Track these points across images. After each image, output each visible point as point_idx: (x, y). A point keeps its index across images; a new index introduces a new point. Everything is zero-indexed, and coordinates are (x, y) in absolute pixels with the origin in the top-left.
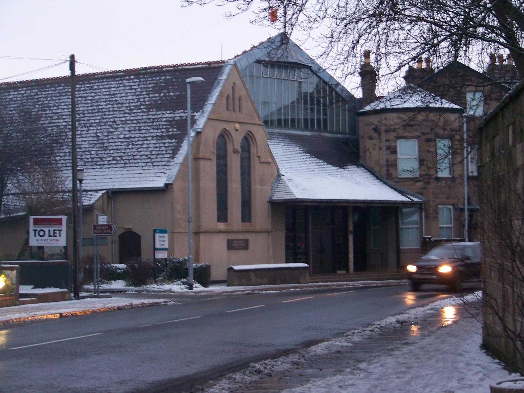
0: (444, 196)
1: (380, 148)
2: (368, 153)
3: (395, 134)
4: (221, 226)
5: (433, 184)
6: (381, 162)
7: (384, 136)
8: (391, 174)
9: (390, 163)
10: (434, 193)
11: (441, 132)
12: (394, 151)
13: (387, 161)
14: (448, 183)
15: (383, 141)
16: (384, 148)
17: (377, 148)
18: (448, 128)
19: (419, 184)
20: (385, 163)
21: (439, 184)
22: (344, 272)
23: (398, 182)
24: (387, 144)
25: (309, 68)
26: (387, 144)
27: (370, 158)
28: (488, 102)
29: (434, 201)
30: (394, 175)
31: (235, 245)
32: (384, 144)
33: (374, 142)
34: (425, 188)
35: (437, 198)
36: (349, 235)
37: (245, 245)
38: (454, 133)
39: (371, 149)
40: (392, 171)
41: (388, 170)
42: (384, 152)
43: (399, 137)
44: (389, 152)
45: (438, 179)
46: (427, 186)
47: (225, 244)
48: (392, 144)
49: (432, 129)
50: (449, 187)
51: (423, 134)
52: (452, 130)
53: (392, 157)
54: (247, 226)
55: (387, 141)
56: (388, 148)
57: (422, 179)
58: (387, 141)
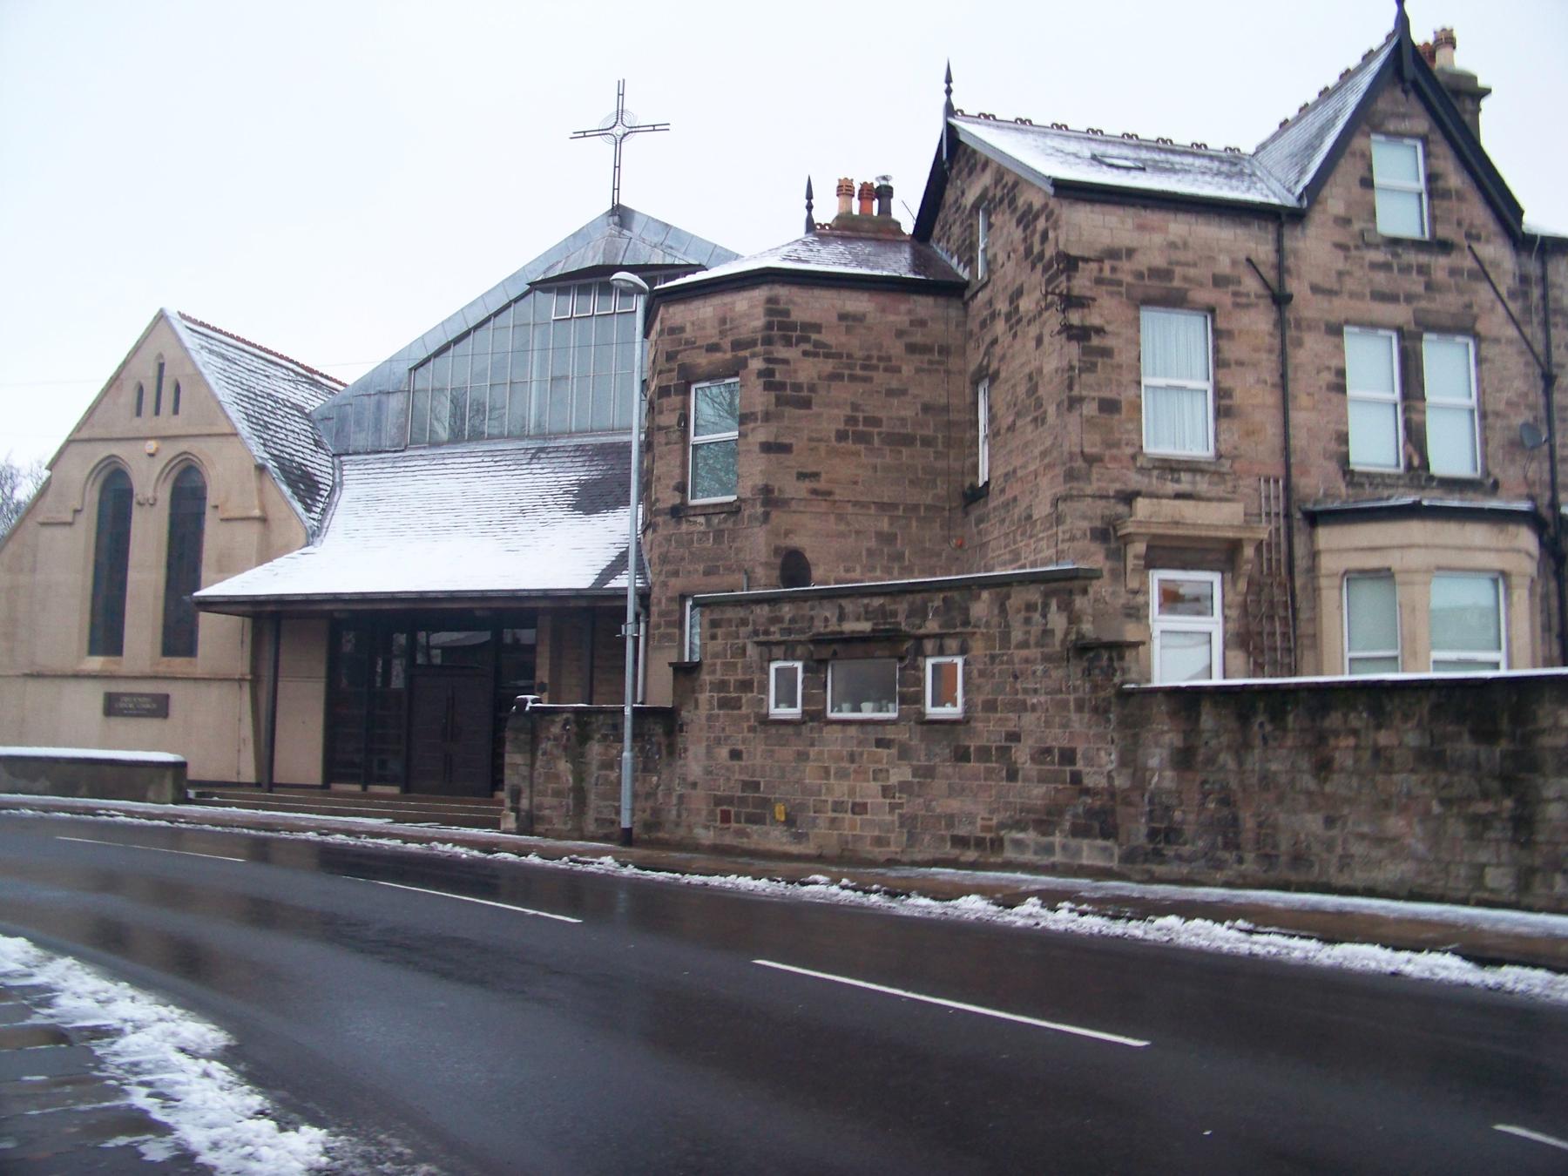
0: (701, 568)
4: (96, 663)
11: (702, 360)
14: (715, 520)
21: (684, 527)
29: (665, 584)
31: (122, 705)
35: (676, 574)
37: (160, 707)
38: (747, 353)
47: (98, 703)
50: (719, 535)
52: (737, 345)
54: (178, 664)
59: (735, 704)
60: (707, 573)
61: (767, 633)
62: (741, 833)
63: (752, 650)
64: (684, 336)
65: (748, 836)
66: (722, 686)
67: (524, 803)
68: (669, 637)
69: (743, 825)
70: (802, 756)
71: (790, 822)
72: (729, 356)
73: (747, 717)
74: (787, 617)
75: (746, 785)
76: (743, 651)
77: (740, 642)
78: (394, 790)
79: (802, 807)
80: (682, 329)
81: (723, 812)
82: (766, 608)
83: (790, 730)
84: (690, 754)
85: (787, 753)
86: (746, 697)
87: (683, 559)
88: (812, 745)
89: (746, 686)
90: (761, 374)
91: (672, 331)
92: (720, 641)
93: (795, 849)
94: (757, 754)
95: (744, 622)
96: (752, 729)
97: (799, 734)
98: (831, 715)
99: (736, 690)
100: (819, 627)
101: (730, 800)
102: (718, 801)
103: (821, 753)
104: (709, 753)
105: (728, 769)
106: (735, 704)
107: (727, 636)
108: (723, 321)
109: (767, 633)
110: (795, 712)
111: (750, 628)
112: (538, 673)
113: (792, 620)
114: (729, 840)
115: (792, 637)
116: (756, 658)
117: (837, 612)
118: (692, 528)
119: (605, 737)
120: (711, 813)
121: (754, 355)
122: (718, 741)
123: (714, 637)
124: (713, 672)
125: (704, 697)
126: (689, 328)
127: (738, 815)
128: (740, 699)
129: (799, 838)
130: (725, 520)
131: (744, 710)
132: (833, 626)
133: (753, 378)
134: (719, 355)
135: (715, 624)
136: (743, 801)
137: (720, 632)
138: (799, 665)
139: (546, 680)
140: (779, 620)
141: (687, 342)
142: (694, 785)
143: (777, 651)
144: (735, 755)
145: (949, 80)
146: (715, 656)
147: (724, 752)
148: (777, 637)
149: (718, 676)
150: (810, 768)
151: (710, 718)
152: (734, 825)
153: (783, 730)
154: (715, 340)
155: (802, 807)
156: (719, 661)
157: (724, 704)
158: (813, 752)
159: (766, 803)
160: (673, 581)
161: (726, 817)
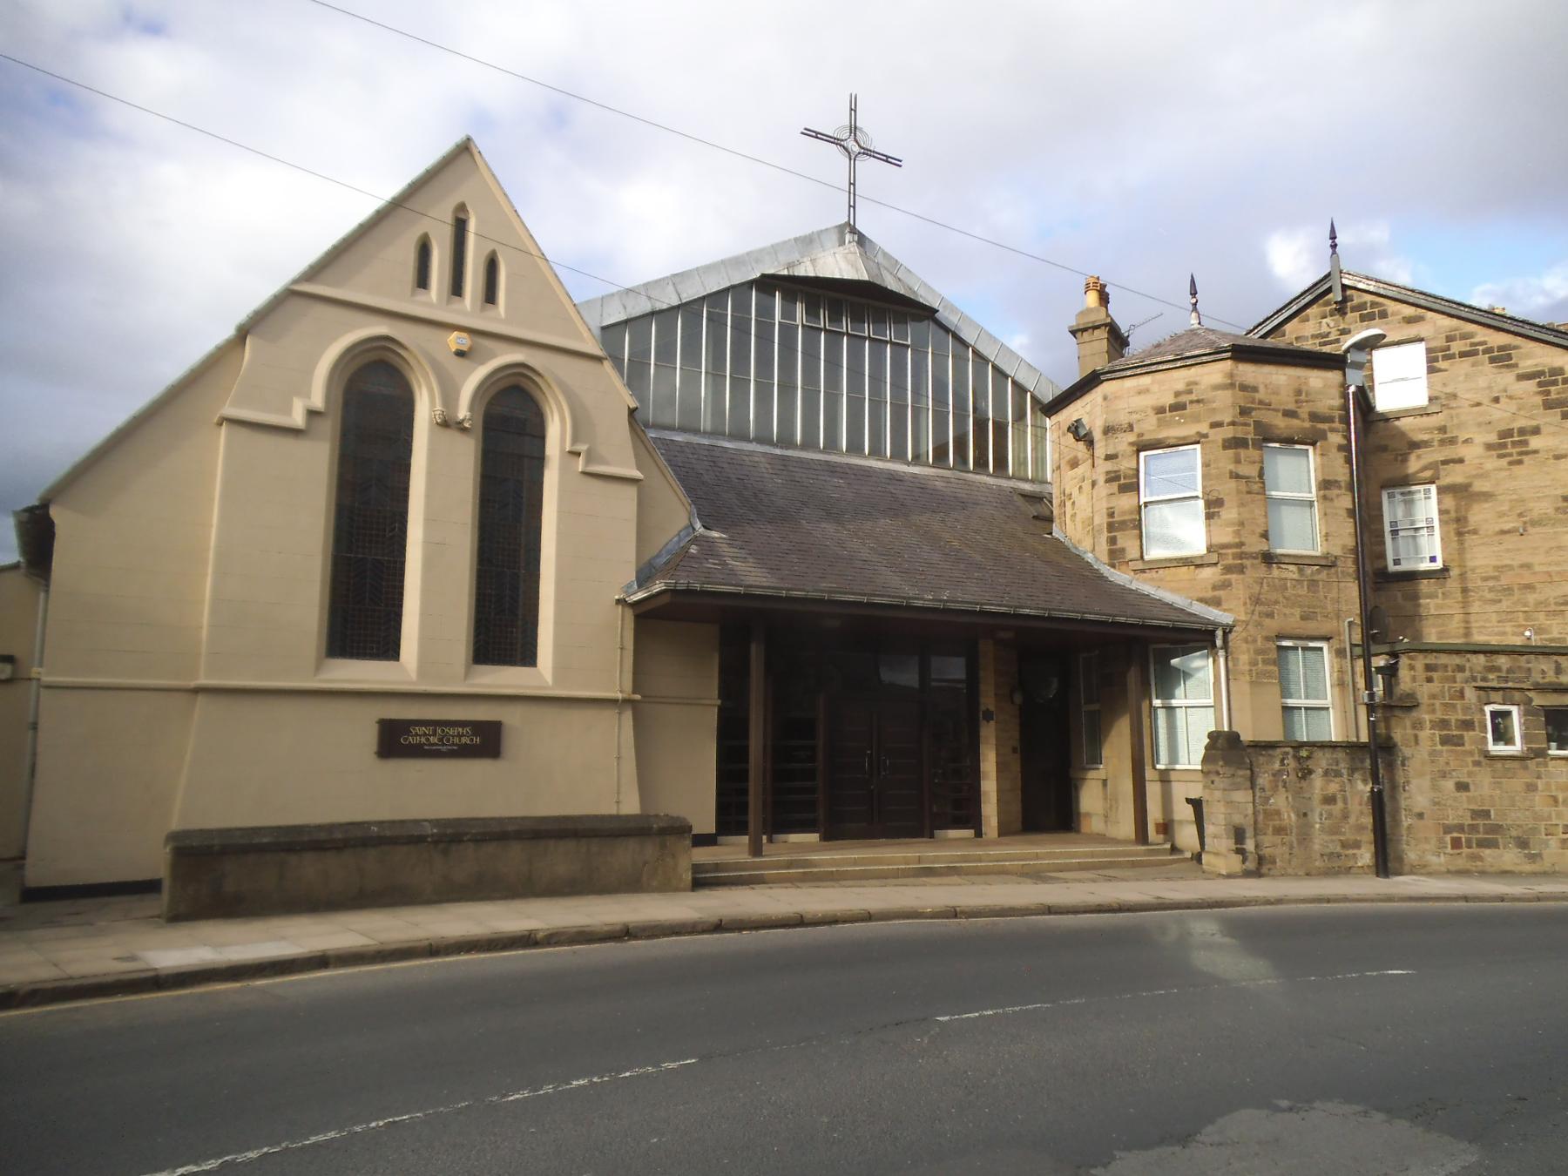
0: (1297, 612)
1: (1094, 484)
2: (1068, 504)
3: (1132, 438)
5: (1256, 571)
6: (1097, 521)
7: (1100, 450)
8: (1123, 550)
9: (1117, 519)
10: (1257, 601)
11: (1281, 423)
12: (1134, 487)
13: (1111, 515)
14: (1308, 571)
15: (1099, 461)
16: (1101, 479)
17: (1087, 485)
18: (1304, 411)
19: (1208, 574)
20: (1105, 520)
21: (1276, 572)
22: (969, 833)
23: (1143, 571)
24: (1110, 466)
25: (926, 313)
26: (1110, 466)
27: (1074, 515)
28: (1441, 364)
29: (1259, 624)
30: (1133, 553)
32: (1103, 467)
33: (1079, 471)
34: (1226, 585)
35: (1270, 615)
36: (983, 724)
38: (1325, 426)
39: (1075, 492)
40: (1126, 541)
41: (1112, 541)
42: (1103, 489)
43: (1141, 447)
44: (1114, 486)
45: (1269, 559)
46: (1233, 577)
48: (1125, 465)
49: (1244, 412)
50: (1313, 584)
51: (1214, 425)
52: (1314, 417)
53: (1126, 502)
55: (1109, 457)
56: (1112, 477)
57: (1214, 558)
58: (1109, 457)
59: (1458, 742)
60: (1303, 618)
61: (1484, 679)
62: (1475, 858)
63: (1470, 694)
64: (1258, 396)
65: (1481, 859)
66: (1444, 724)
67: (1250, 845)
68: (1268, 675)
69: (1475, 850)
70: (1531, 788)
71: (1523, 844)
72: (1307, 424)
73: (1471, 753)
74: (1504, 668)
75: (1476, 814)
76: (1462, 695)
77: (1458, 686)
78: (813, 837)
79: (1534, 830)
80: (1255, 389)
81: (1453, 839)
82: (1482, 658)
83: (1516, 764)
84: (1412, 787)
85: (1517, 784)
86: (1468, 735)
87: (1276, 602)
88: (1539, 777)
89: (1467, 725)
90: (1340, 448)
91: (1244, 388)
92: (1436, 684)
93: (1528, 868)
94: (1484, 784)
95: (1461, 669)
96: (1477, 764)
97: (1526, 768)
98: (1553, 752)
99: (1457, 728)
100: (1537, 677)
101: (1460, 828)
102: (1448, 829)
103: (1548, 784)
104: (1435, 788)
105: (1455, 799)
106: (1458, 742)
107: (1447, 679)
108: (1299, 392)
109: (1484, 679)
110: (1517, 747)
111: (1467, 674)
112: (982, 700)
113: (1509, 671)
114: (1461, 863)
115: (1510, 685)
116: (1474, 700)
117: (1553, 666)
118: (1284, 575)
119: (1326, 773)
120: (1441, 841)
121: (1333, 430)
122: (1444, 775)
123: (1430, 680)
124: (1433, 711)
125: (1425, 734)
126: (1262, 389)
127: (1469, 841)
128: (1462, 737)
129: (1533, 858)
130: (1318, 572)
131: (1467, 747)
132: (1551, 677)
133: (1334, 450)
134: (1295, 422)
135: (1429, 668)
136: (1473, 828)
137: (1435, 675)
138: (1488, 709)
139: (992, 708)
140: (1498, 669)
141: (1261, 402)
142: (1420, 816)
143: (1494, 696)
144: (1462, 787)
145: (1333, 237)
146: (1433, 697)
147: (1450, 785)
148: (1495, 684)
149: (1439, 715)
150: (1539, 801)
151: (1433, 753)
152: (1465, 851)
153: (1509, 764)
154: (1291, 406)
155: (1534, 830)
156: (1437, 703)
157: (1445, 741)
158: (1540, 783)
159: (1496, 829)
160: (1267, 621)
161: (1456, 844)
